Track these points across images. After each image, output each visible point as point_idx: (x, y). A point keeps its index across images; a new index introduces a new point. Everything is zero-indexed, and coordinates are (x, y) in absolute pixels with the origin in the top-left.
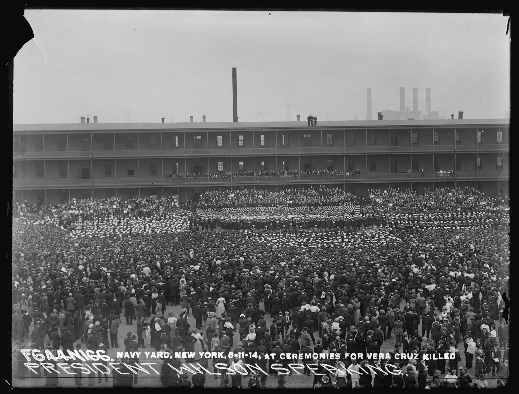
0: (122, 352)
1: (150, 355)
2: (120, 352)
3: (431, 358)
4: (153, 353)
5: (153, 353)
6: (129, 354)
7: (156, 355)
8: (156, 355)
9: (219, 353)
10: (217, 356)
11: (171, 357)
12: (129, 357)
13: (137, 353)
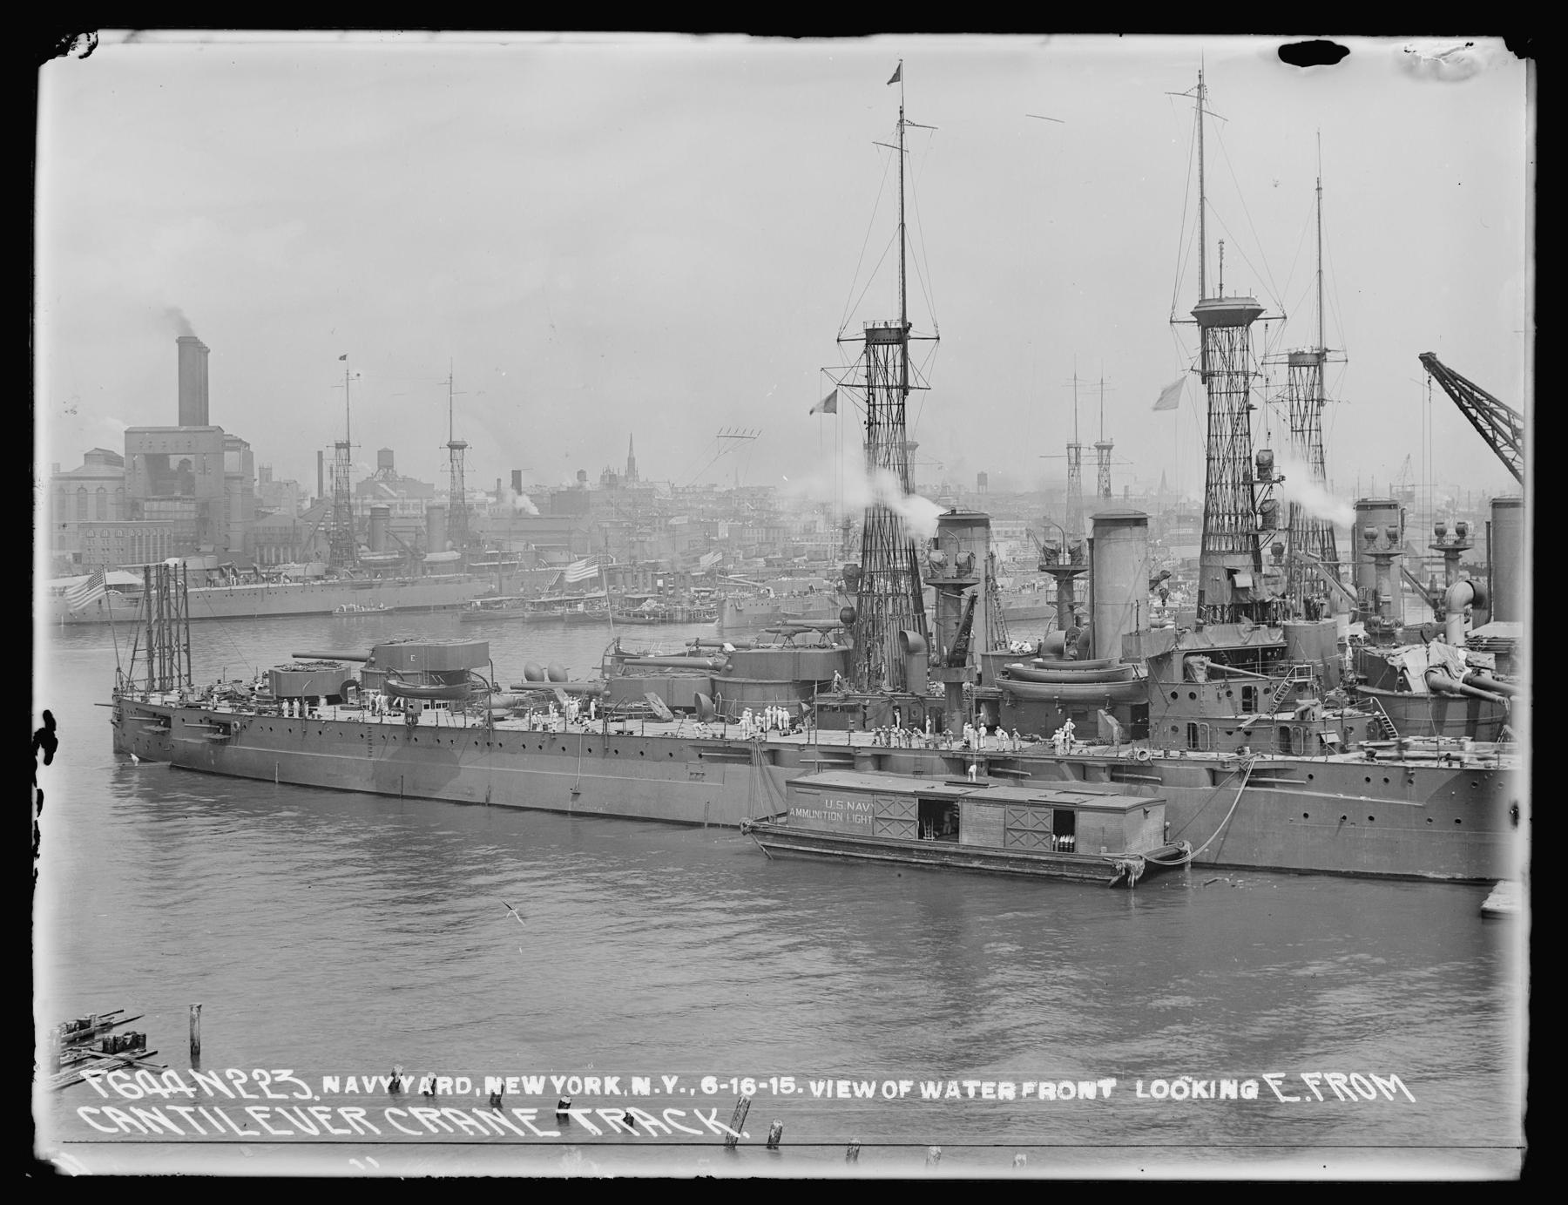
2: (330, 1078)
3: (1213, 1096)
6: (362, 1087)
9: (607, 1079)
10: (602, 1088)
11: (478, 1092)
12: (355, 1088)
13: (382, 1079)
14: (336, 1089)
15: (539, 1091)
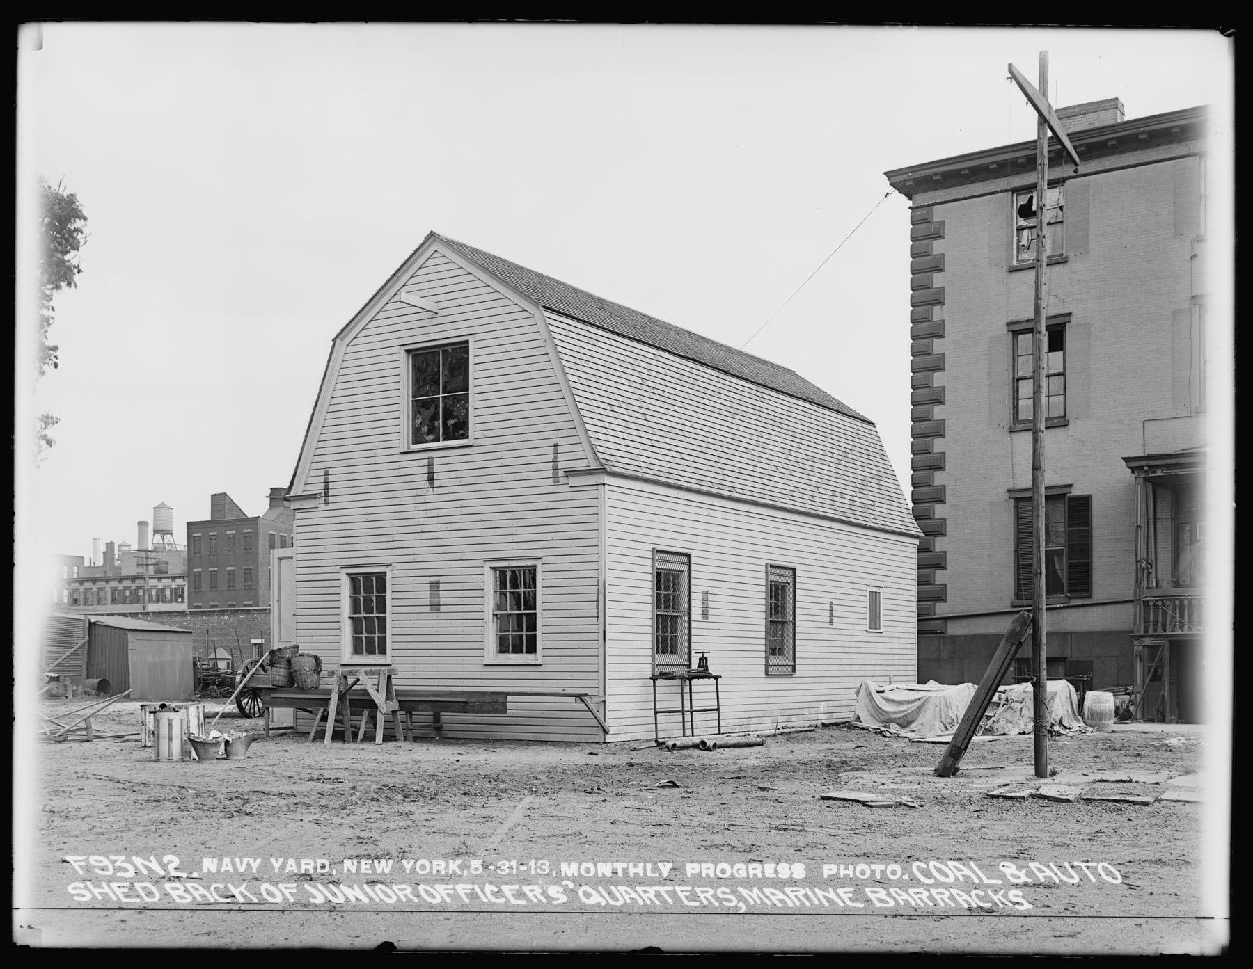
0: (215, 860)
1: (283, 867)
4: (291, 862)
5: (291, 862)
6: (235, 868)
7: (299, 866)
8: (299, 866)
9: (451, 862)
12: (232, 871)
13: (251, 861)
14: (214, 870)
15: (387, 871)
